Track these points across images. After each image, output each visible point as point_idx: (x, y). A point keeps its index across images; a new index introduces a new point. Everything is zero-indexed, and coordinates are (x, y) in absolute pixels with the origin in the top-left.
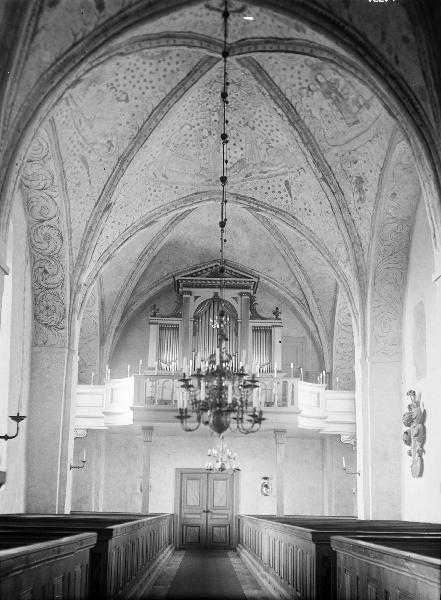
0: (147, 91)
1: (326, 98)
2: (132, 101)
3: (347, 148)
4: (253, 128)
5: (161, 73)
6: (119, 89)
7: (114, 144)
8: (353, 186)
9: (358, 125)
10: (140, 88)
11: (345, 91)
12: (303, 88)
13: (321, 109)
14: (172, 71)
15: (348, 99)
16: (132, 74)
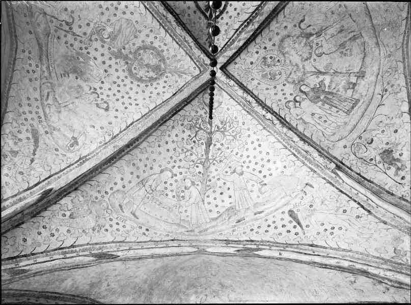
0: (129, 107)
2: (112, 112)
3: (355, 135)
4: (242, 174)
5: (147, 94)
6: (101, 97)
7: (80, 143)
8: (381, 166)
9: (359, 104)
10: (123, 103)
11: (333, 86)
12: (289, 101)
13: (313, 114)
14: (158, 94)
15: (338, 91)
16: (119, 89)
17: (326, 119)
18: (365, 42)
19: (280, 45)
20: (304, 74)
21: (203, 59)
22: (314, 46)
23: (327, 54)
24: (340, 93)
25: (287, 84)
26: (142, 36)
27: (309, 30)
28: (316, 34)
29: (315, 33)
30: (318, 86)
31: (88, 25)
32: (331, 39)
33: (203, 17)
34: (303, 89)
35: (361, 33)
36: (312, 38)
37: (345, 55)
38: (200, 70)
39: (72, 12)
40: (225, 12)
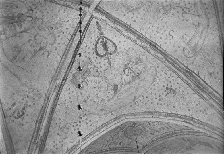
1: (19, 14)
11: (13, 28)
13: (17, 7)
15: (8, 26)
17: (8, 8)
18: (8, 58)
19: (55, 38)
20: (33, 27)
21: (99, 15)
22: (35, 45)
23: (25, 43)
24: (7, 26)
25: (41, 17)
26: (140, 17)
27: (42, 51)
28: (37, 52)
29: (38, 52)
30: (22, 24)
31: (173, 14)
32: (27, 52)
33: (107, 36)
34: (30, 18)
35: (12, 62)
36: (39, 48)
37: (15, 47)
38: (99, 7)
39: (183, 20)
40: (95, 44)
